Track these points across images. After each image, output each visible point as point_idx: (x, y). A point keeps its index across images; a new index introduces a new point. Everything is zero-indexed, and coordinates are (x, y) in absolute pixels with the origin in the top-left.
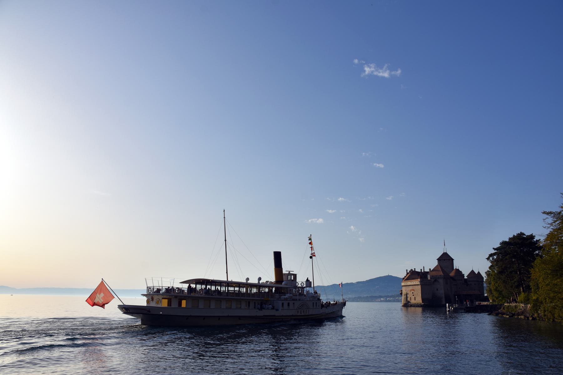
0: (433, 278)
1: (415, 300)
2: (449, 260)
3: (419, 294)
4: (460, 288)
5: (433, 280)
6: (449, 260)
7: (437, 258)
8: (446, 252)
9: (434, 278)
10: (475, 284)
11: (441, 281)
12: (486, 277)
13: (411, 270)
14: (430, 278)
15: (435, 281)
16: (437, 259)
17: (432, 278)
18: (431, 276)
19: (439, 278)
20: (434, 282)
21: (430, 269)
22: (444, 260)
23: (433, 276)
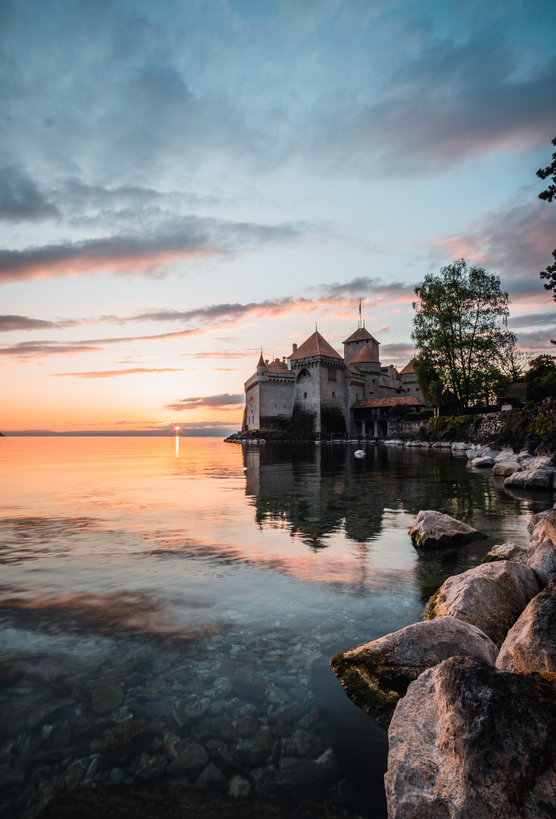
0: (297, 365)
1: (253, 423)
2: (367, 341)
3: (257, 407)
4: (371, 393)
5: (297, 372)
6: (367, 341)
7: (344, 339)
8: (362, 327)
9: (299, 365)
11: (315, 371)
12: (420, 308)
13: (277, 360)
14: (292, 367)
15: (304, 373)
17: (295, 366)
18: (293, 360)
19: (309, 363)
20: (299, 376)
21: (295, 346)
22: (357, 342)
23: (297, 360)
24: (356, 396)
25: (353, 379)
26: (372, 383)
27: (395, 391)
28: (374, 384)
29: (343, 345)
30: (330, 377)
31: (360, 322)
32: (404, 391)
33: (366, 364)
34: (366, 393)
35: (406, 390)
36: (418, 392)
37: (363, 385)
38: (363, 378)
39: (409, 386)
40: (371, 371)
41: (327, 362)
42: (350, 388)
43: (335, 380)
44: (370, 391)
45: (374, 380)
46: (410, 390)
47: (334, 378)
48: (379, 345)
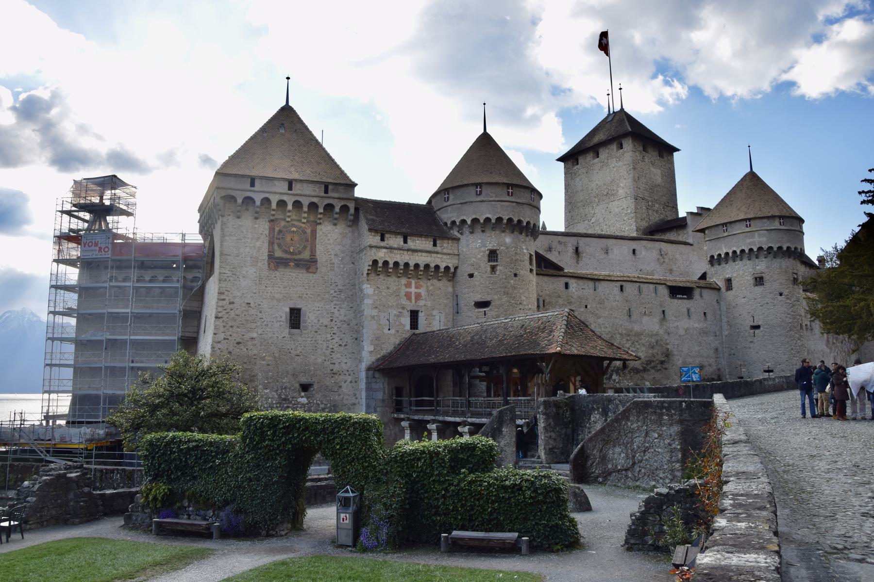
8: (617, 108)
10: (759, 281)
16: (559, 160)
24: (406, 321)
25: (382, 255)
26: (486, 266)
27: (664, 291)
28: (493, 268)
29: (562, 164)
30: (278, 253)
31: (610, 93)
32: (719, 289)
33: (459, 192)
34: (462, 303)
35: (721, 284)
36: (759, 289)
37: (450, 274)
38: (445, 246)
39: (730, 270)
40: (475, 221)
41: (258, 198)
42: (368, 289)
43: (309, 264)
44: (479, 298)
45: (493, 255)
46: (734, 284)
47: (306, 255)
48: (675, 154)
